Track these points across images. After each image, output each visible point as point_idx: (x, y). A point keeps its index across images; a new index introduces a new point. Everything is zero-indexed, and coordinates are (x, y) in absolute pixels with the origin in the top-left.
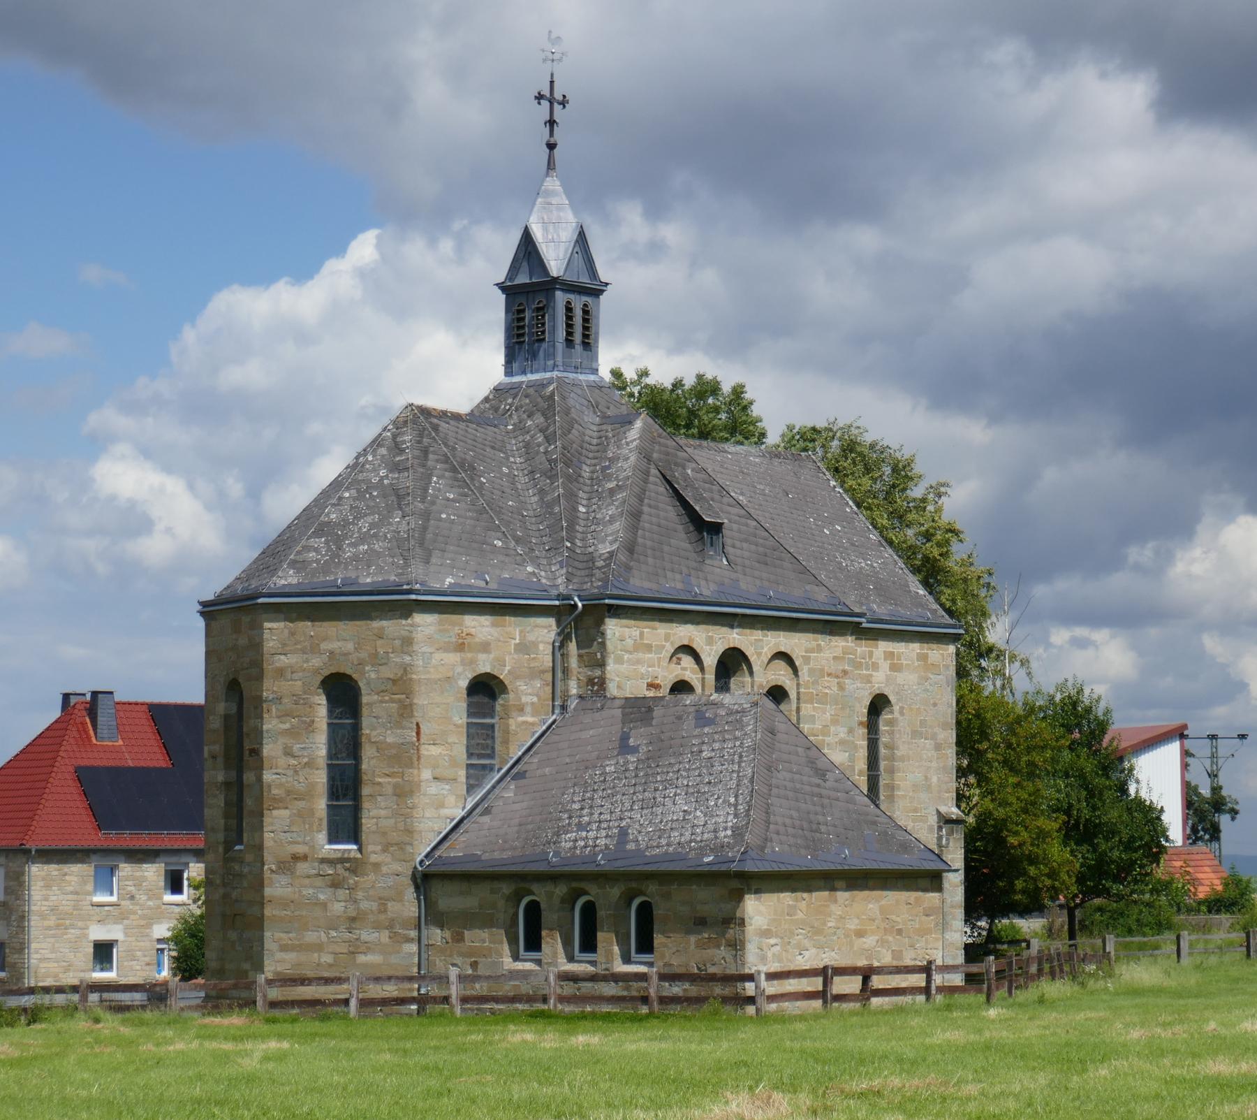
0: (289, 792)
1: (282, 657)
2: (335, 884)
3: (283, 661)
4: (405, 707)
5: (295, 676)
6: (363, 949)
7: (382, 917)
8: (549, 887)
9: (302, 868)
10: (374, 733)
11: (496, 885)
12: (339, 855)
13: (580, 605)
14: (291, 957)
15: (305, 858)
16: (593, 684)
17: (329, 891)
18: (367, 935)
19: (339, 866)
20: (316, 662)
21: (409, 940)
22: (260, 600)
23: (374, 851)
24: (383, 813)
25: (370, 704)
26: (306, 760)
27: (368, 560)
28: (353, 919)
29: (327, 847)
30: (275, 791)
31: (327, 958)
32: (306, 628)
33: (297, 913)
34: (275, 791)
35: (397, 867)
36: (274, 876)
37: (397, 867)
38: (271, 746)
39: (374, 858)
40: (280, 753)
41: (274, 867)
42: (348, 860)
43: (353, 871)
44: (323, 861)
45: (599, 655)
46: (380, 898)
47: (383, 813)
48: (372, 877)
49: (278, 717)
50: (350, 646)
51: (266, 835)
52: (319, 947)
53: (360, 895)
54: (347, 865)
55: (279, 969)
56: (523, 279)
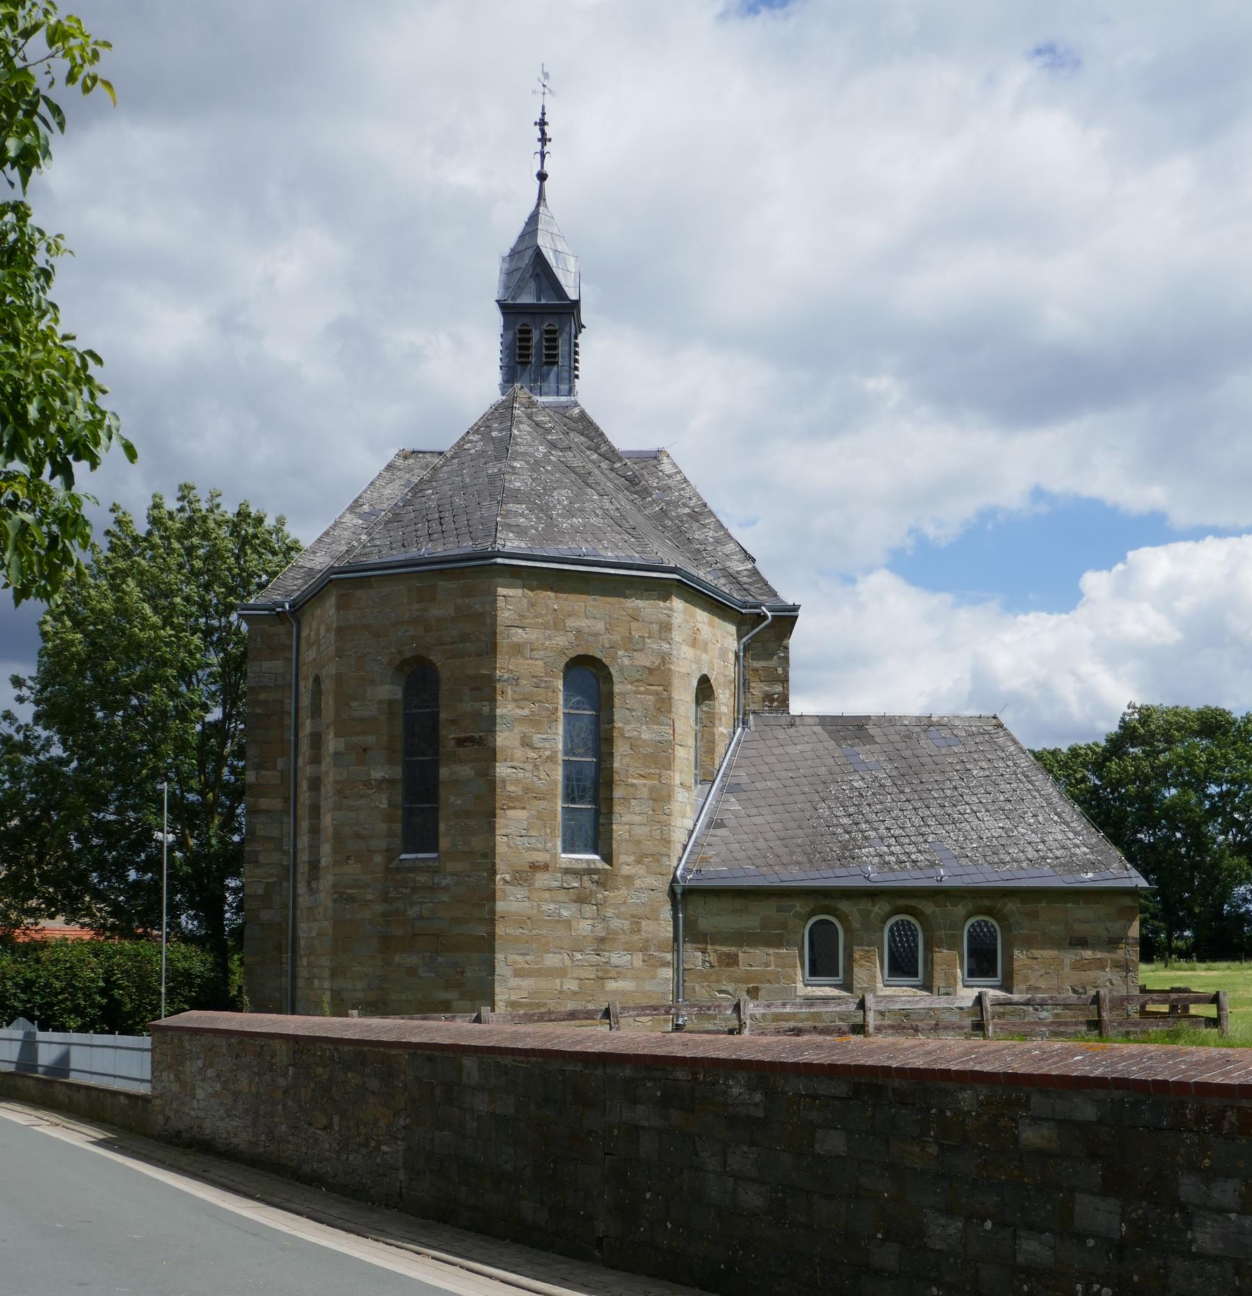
0: (527, 790)
1: (520, 631)
2: (582, 899)
3: (519, 635)
4: (663, 700)
5: (536, 654)
6: (613, 974)
7: (636, 937)
8: (865, 904)
9: (542, 879)
10: (628, 728)
11: (785, 902)
12: (585, 866)
13: (769, 614)
14: (527, 983)
15: (545, 868)
16: (772, 700)
17: (574, 906)
18: (618, 958)
19: (585, 878)
20: (561, 640)
21: (665, 964)
22: (499, 560)
23: (625, 861)
24: (637, 819)
25: (623, 695)
26: (548, 753)
27: (597, 535)
28: (602, 940)
29: (563, 855)
30: (510, 788)
31: (571, 985)
32: (549, 599)
33: (535, 932)
34: (510, 788)
35: (651, 881)
36: (508, 887)
37: (651, 881)
38: (506, 734)
39: (626, 870)
40: (517, 743)
41: (508, 877)
42: (596, 871)
43: (602, 884)
44: (567, 871)
45: (780, 671)
46: (633, 916)
47: (637, 819)
48: (624, 891)
49: (514, 700)
50: (600, 626)
51: (498, 838)
52: (561, 972)
53: (609, 912)
54: (596, 877)
55: (513, 998)
56: (527, 299)
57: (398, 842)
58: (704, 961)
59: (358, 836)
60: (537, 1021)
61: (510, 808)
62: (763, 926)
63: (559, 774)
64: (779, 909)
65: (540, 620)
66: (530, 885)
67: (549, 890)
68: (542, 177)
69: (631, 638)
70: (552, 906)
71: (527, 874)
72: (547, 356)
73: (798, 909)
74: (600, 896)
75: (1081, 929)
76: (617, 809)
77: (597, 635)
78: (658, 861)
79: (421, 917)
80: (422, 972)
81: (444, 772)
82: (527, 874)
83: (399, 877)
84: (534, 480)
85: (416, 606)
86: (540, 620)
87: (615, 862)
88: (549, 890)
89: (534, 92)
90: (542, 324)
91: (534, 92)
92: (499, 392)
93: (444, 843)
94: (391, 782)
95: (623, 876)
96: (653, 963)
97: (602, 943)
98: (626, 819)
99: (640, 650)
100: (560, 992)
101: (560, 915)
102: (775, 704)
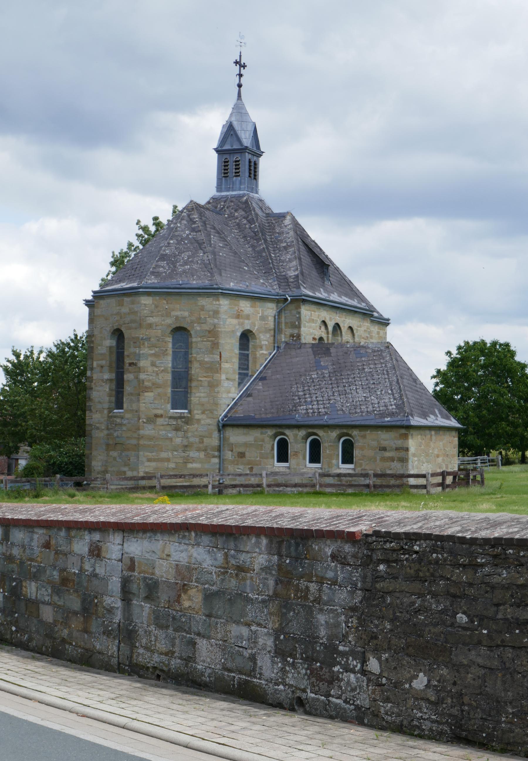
0: (153, 384)
1: (151, 318)
2: (177, 429)
3: (151, 320)
4: (214, 344)
5: (158, 328)
6: (191, 461)
8: (295, 431)
9: (160, 421)
10: (198, 356)
11: (264, 430)
12: (179, 415)
13: (289, 298)
14: (153, 464)
15: (161, 416)
16: (293, 337)
17: (174, 432)
18: (193, 454)
19: (179, 420)
20: (169, 321)
21: (214, 457)
24: (202, 395)
25: (197, 342)
26: (162, 368)
27: (192, 273)
28: (186, 446)
29: (171, 411)
30: (146, 384)
32: (164, 303)
33: (156, 443)
34: (146, 384)
35: (209, 421)
36: (145, 425)
37: (209, 421)
38: (144, 361)
39: (197, 417)
40: (149, 365)
41: (145, 420)
42: (184, 417)
43: (187, 423)
44: (171, 418)
45: (297, 323)
46: (200, 436)
47: (202, 395)
48: (196, 426)
49: (148, 347)
50: (186, 314)
51: (141, 404)
52: (168, 460)
53: (190, 434)
54: (183, 420)
55: (147, 470)
56: (227, 147)
57: (113, 405)
58: (232, 455)
59: (100, 402)
60: (130, 480)
61: (146, 392)
62: (255, 441)
63: (169, 377)
64: (262, 433)
65: (160, 313)
66: (155, 423)
67: (163, 425)
68: (240, 86)
69: (200, 318)
70: (164, 432)
71: (152, 419)
72: (236, 173)
73: (269, 433)
74: (185, 428)
75: (384, 443)
76: (194, 391)
77: (185, 318)
78: (212, 413)
79: (118, 437)
80: (118, 459)
81: (125, 376)
82: (152, 419)
83: (111, 420)
84: (176, 248)
85: (118, 308)
86: (160, 313)
87: (192, 413)
88: (163, 425)
89: (236, 46)
90: (233, 157)
91: (236, 46)
92: (215, 189)
93: (125, 406)
94: (111, 380)
95: (196, 419)
96: (208, 456)
97: (186, 447)
98: (197, 395)
99: (205, 323)
100: (167, 468)
101: (167, 436)
102: (295, 338)
